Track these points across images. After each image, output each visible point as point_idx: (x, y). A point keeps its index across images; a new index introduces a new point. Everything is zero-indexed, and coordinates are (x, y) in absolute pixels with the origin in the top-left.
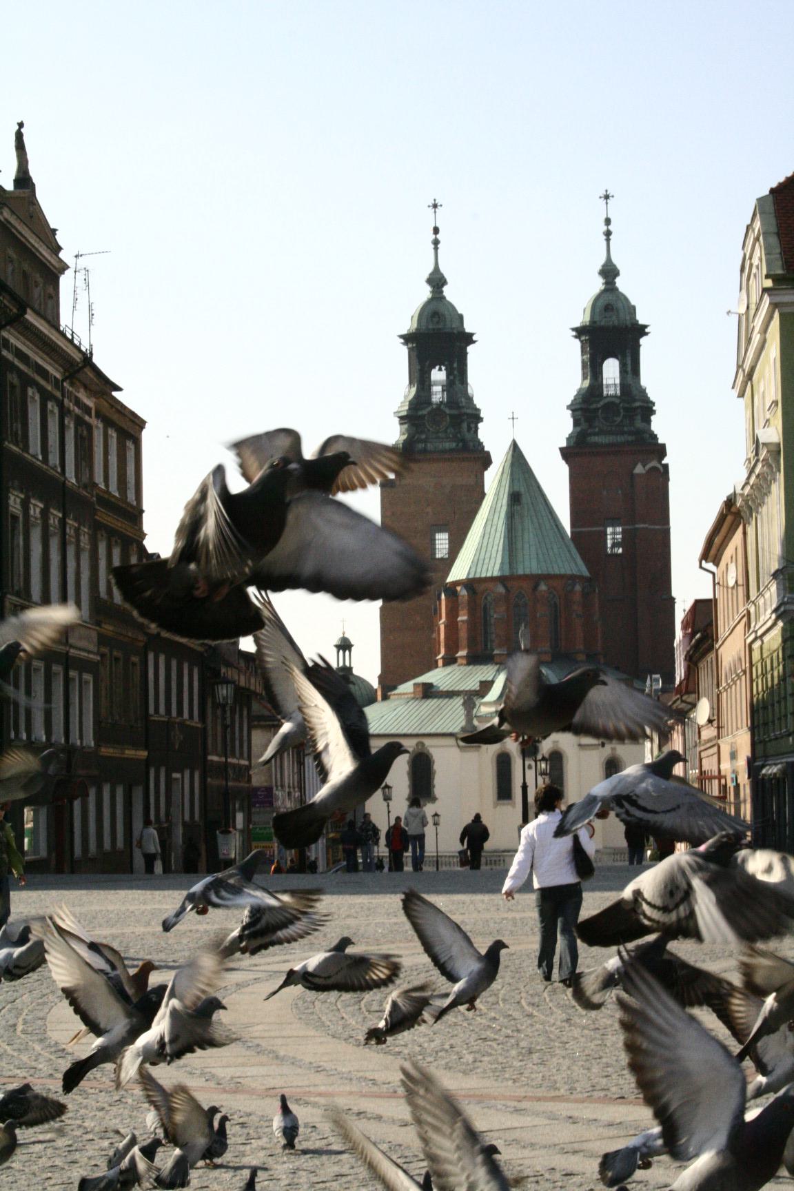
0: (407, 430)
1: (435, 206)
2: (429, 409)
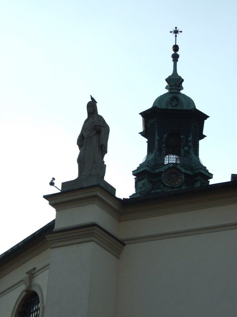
0: (144, 184)
1: (176, 32)
2: (167, 167)
